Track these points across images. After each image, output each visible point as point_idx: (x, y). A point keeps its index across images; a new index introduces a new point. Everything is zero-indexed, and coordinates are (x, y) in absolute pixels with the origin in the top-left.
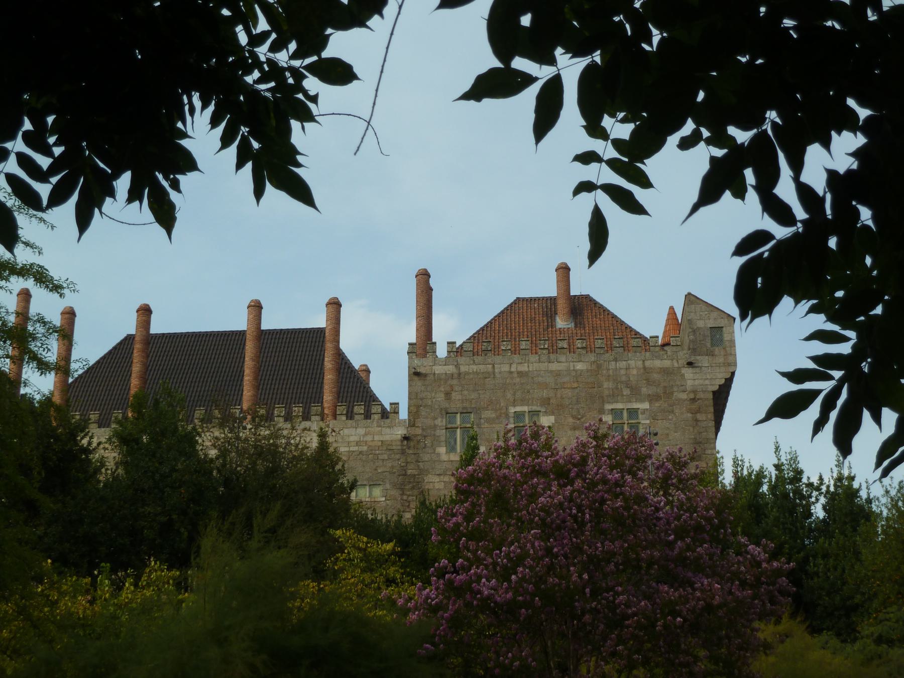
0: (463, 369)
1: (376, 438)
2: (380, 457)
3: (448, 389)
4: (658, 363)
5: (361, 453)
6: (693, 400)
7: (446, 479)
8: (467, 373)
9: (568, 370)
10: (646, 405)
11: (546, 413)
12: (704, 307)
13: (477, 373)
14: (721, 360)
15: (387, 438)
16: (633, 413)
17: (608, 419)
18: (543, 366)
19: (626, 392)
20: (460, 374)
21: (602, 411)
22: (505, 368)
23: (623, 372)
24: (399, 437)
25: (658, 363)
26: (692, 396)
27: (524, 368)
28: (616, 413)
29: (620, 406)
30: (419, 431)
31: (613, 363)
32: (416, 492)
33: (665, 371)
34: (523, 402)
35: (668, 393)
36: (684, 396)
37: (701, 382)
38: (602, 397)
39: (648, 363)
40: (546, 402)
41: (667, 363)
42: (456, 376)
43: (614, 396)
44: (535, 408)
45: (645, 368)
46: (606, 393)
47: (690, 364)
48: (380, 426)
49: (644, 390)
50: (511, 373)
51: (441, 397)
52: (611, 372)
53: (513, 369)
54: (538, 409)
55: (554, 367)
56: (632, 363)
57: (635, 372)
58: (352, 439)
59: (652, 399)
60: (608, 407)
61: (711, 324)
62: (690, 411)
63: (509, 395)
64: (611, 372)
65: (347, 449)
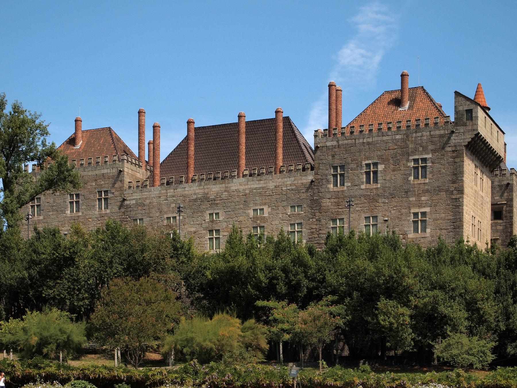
0: (340, 143)
1: (299, 182)
2: (302, 191)
3: (333, 153)
5: (292, 190)
7: (332, 200)
8: (343, 145)
9: (392, 139)
10: (429, 156)
11: (381, 164)
12: (463, 99)
13: (348, 144)
14: (470, 128)
15: (305, 181)
16: (424, 160)
17: (412, 164)
19: (421, 149)
20: (339, 146)
21: (408, 161)
22: (361, 141)
23: (419, 138)
24: (310, 181)
26: (454, 149)
27: (370, 140)
28: (416, 161)
29: (416, 157)
30: (319, 177)
31: (415, 134)
32: (318, 208)
37: (459, 141)
38: (408, 153)
39: (432, 133)
40: (380, 157)
42: (337, 147)
44: (375, 161)
45: (430, 135)
46: (410, 150)
48: (301, 175)
50: (364, 143)
51: (330, 157)
52: (413, 139)
53: (365, 141)
54: (377, 161)
56: (424, 133)
57: (425, 138)
58: (288, 183)
59: (434, 151)
60: (411, 158)
61: (466, 108)
62: (453, 157)
64: (413, 139)
65: (286, 188)
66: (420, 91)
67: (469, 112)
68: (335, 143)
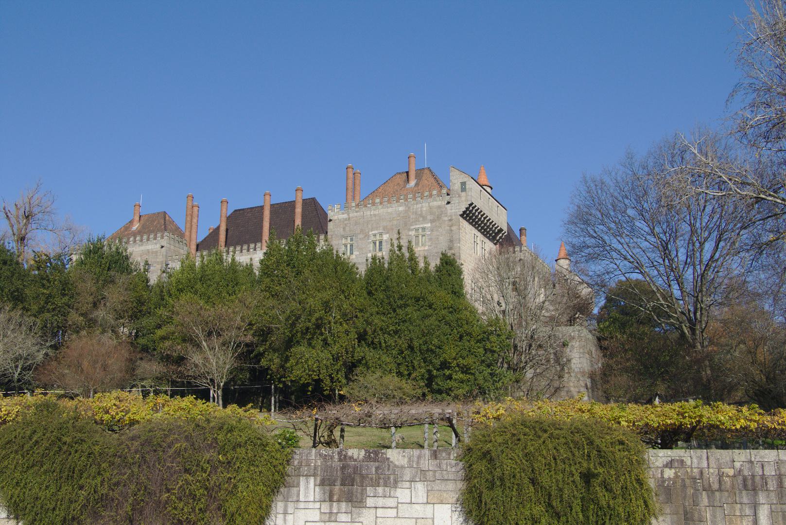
4: (435, 204)
6: (450, 220)
10: (429, 225)
16: (424, 229)
18: (385, 210)
19: (421, 219)
21: (410, 230)
25: (435, 204)
27: (376, 212)
29: (417, 226)
33: (439, 207)
34: (377, 228)
35: (439, 217)
36: (446, 219)
41: (439, 203)
43: (416, 221)
47: (448, 203)
49: (429, 217)
55: (390, 210)
59: (432, 221)
63: (370, 226)
66: (426, 171)
67: (463, 184)
68: (345, 216)
